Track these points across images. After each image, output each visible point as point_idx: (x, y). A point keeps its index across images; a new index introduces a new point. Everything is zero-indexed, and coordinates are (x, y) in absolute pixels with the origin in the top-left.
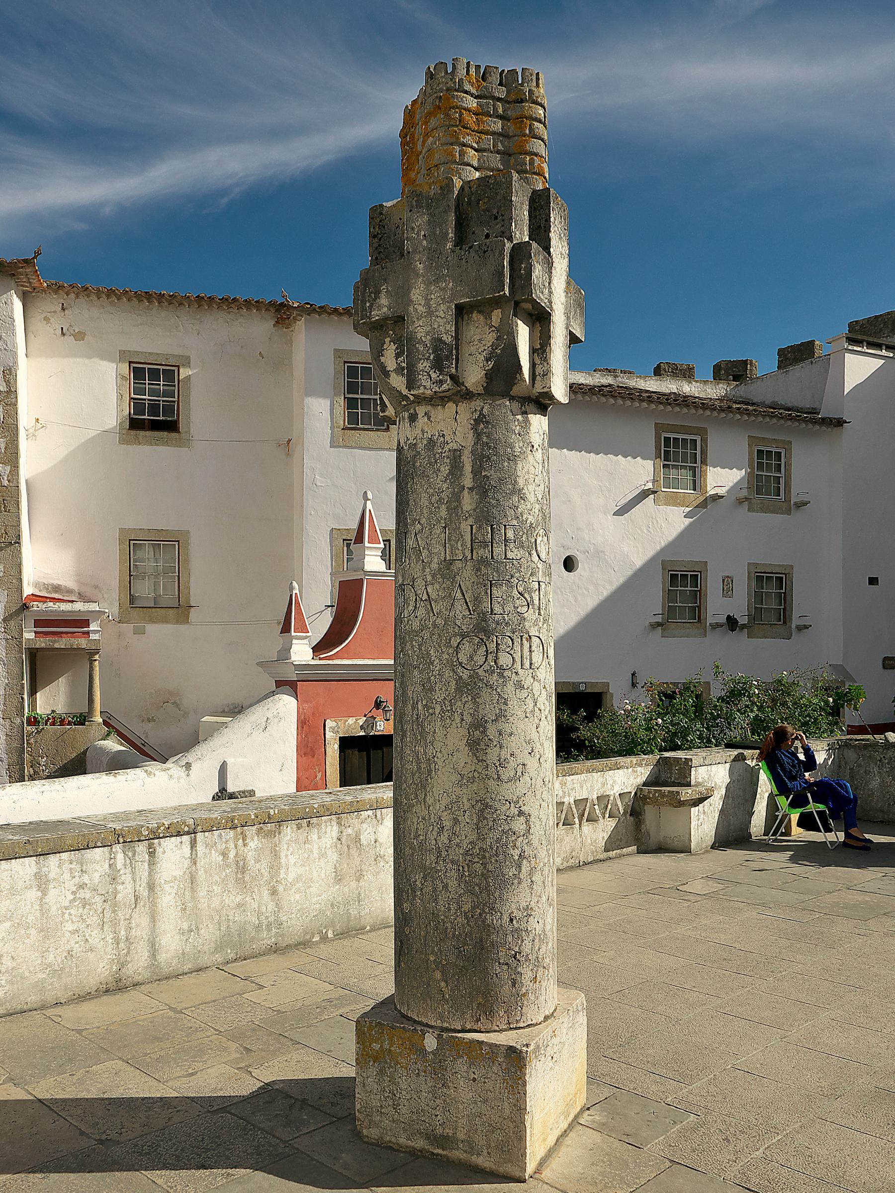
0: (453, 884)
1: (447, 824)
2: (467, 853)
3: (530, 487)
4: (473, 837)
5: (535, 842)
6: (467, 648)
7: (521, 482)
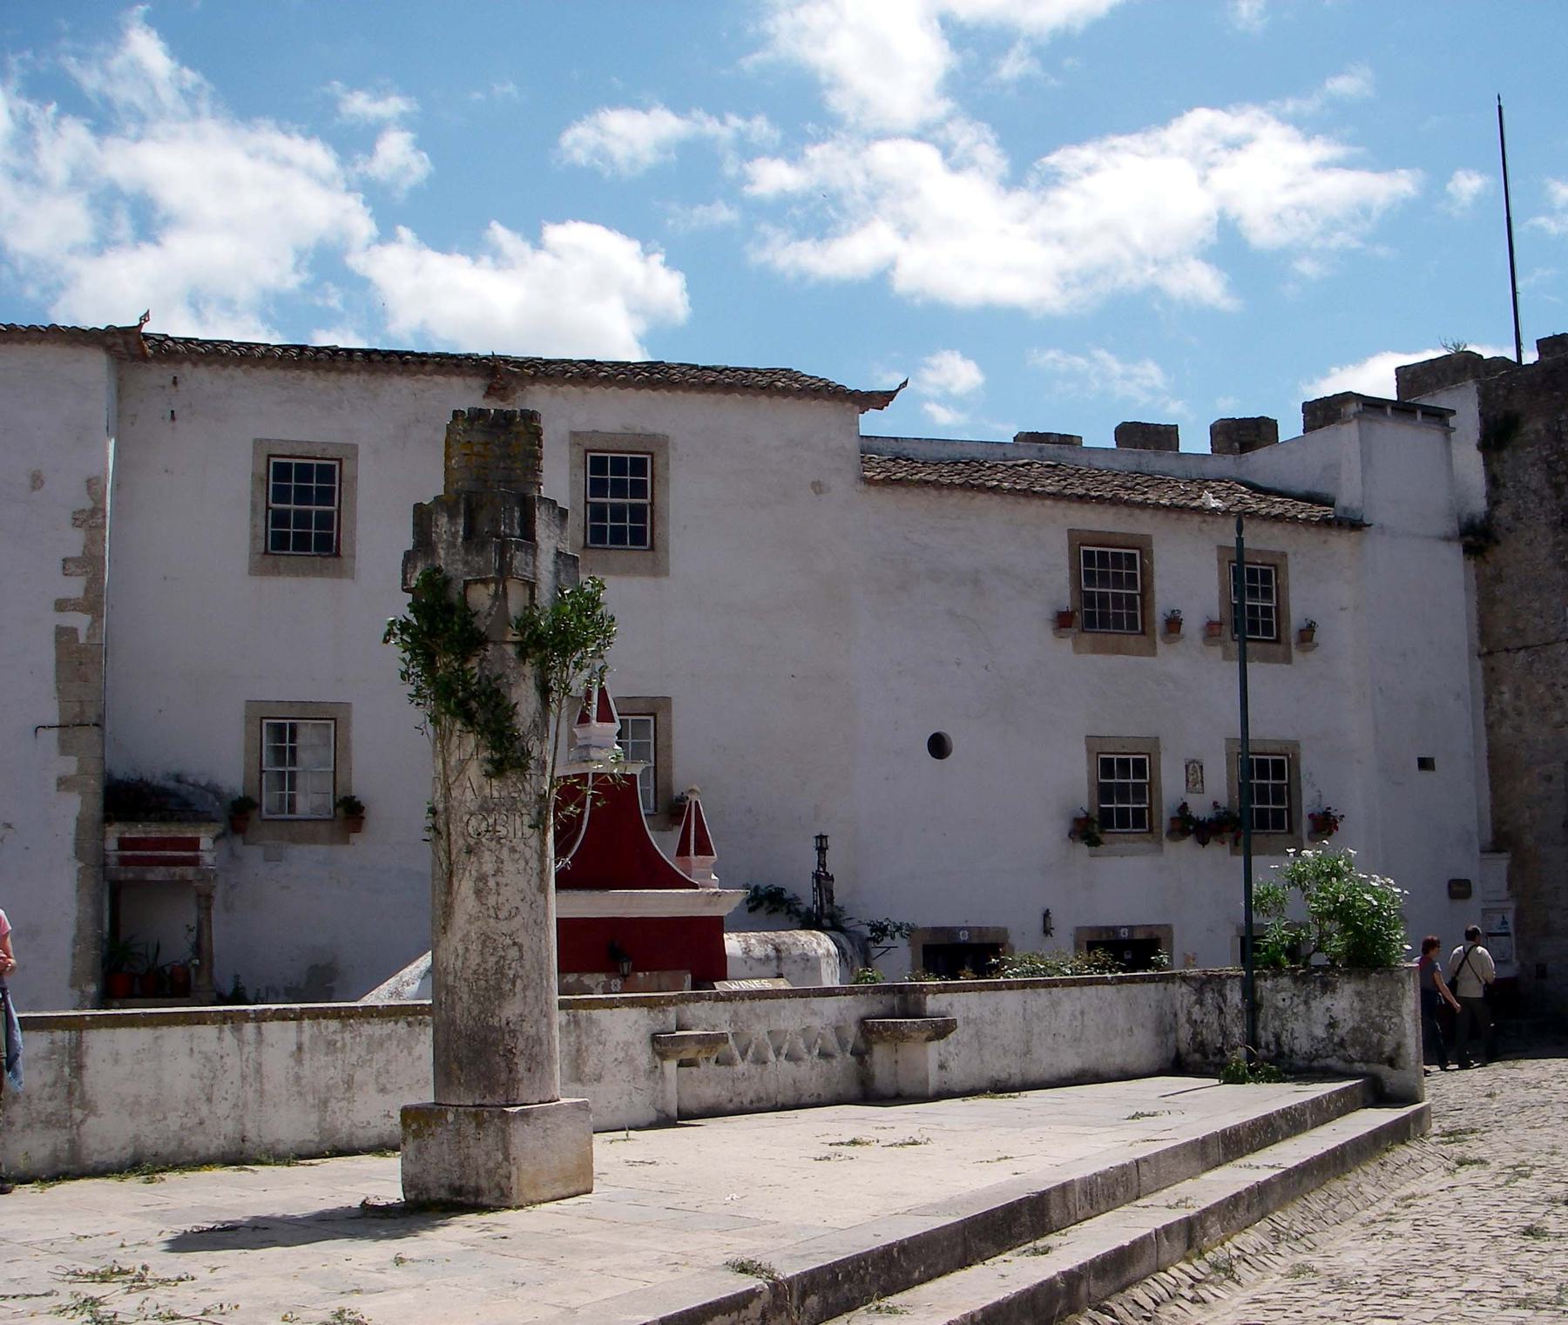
0: (465, 997)
1: (461, 952)
2: (475, 972)
4: (478, 960)
6: (473, 822)
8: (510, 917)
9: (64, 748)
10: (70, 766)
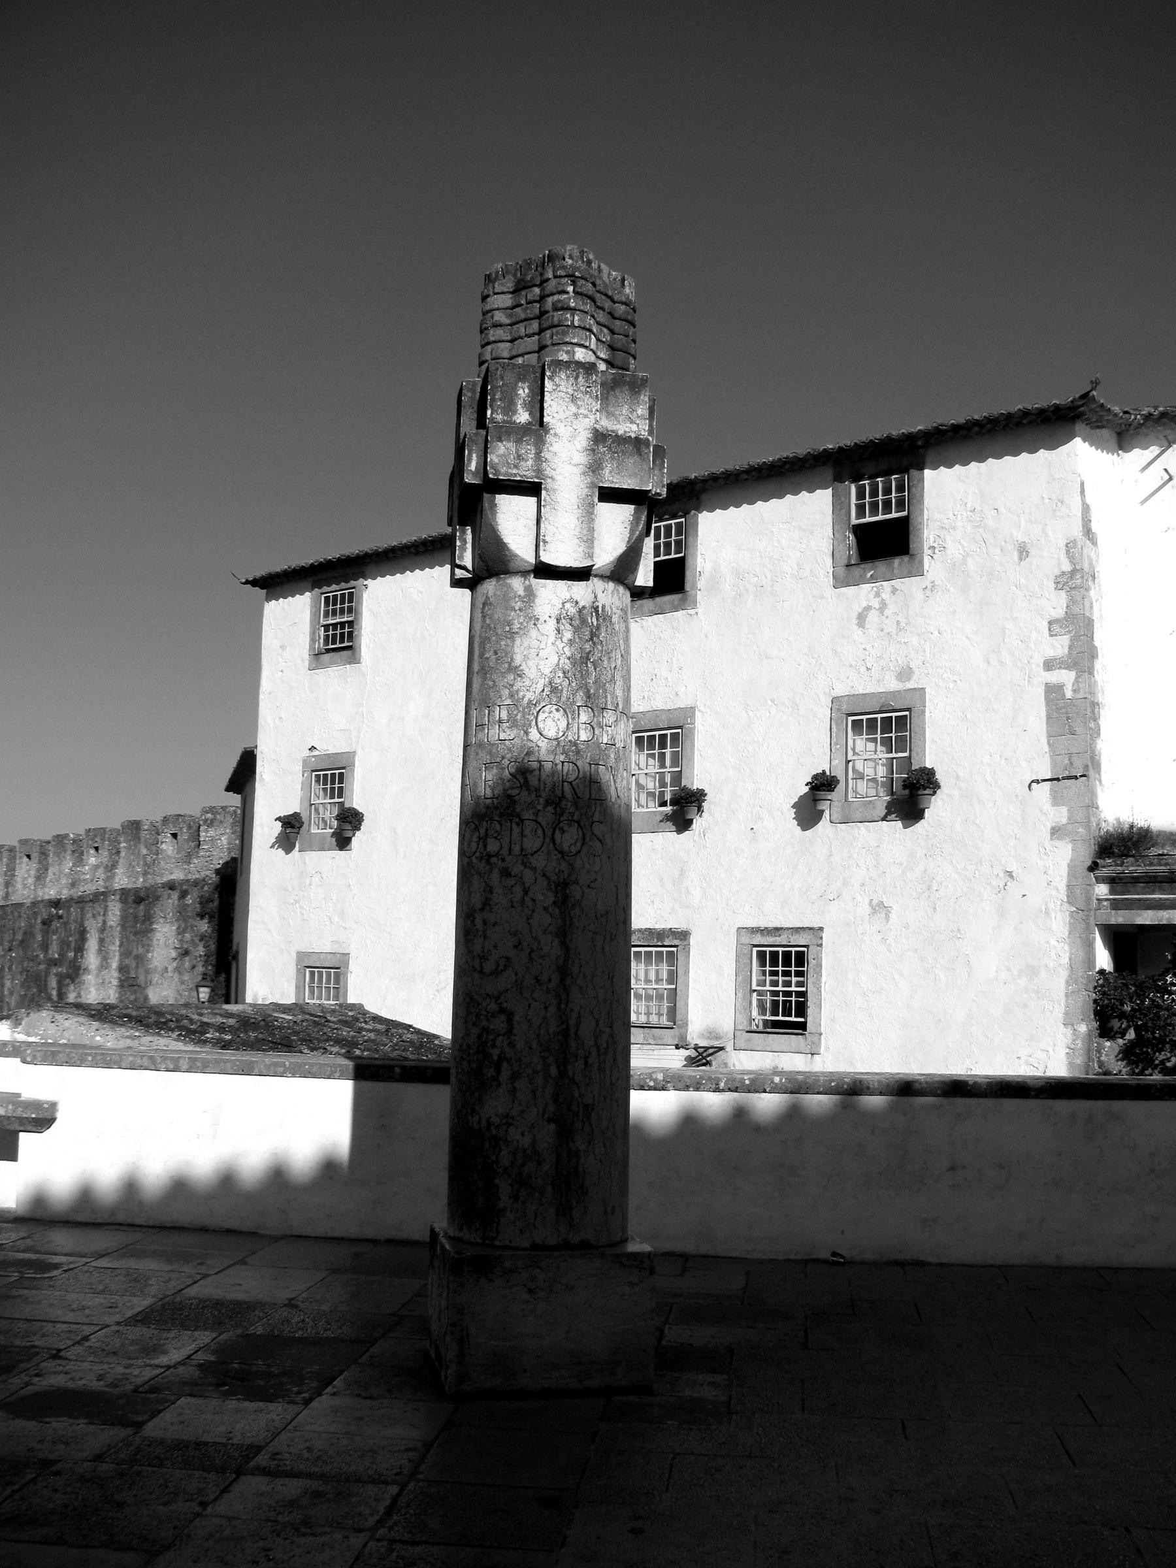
3: (530, 663)
5: (520, 1045)
7: (518, 659)
8: (496, 972)
9: (1056, 800)
10: (1061, 815)
